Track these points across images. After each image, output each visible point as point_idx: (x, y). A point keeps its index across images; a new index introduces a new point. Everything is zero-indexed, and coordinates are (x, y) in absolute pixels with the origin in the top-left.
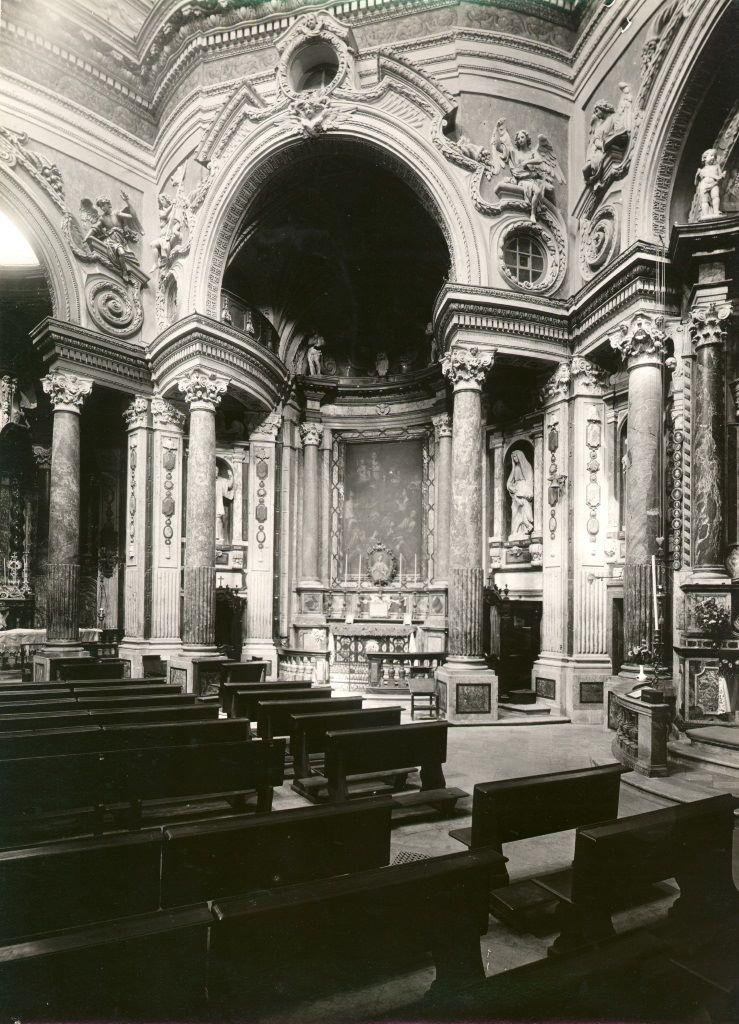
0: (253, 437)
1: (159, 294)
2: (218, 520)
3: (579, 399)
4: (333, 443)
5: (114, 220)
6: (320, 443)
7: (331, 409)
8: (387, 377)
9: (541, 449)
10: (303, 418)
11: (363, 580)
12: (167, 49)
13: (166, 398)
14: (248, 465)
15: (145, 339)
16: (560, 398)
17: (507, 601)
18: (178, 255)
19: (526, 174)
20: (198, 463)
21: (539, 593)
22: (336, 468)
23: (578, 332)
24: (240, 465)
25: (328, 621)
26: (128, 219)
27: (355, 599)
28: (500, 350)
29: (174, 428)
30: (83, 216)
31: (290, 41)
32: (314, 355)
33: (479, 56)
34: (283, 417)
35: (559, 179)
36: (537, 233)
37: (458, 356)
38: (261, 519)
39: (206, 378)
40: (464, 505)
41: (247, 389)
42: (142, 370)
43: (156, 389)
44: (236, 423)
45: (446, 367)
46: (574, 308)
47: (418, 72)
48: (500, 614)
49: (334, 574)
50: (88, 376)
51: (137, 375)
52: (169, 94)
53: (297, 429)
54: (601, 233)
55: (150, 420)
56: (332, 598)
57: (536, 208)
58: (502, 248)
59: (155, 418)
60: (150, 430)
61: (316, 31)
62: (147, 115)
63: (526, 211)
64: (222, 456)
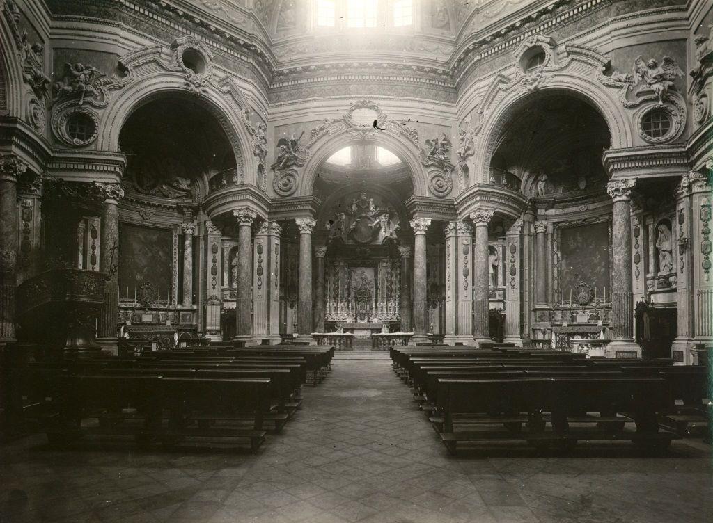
0: (508, 233)
1: (460, 172)
2: (490, 276)
3: (694, 195)
4: (554, 230)
5: (439, 145)
6: (546, 231)
7: (551, 212)
8: (585, 190)
9: (676, 226)
10: (535, 219)
11: (573, 303)
12: (462, 63)
13: (464, 221)
14: (505, 247)
15: (454, 195)
16: (684, 195)
17: (653, 309)
18: (468, 155)
19: (654, 81)
20: (480, 251)
21: (675, 304)
22: (556, 243)
23: (693, 158)
24: (501, 248)
25: (552, 326)
26: (446, 144)
27: (568, 314)
28: (640, 177)
29: (468, 234)
30: (427, 147)
31: (520, 50)
32: (541, 185)
33: (624, 28)
34: (524, 221)
35: (680, 75)
36: (665, 109)
37: (614, 185)
38: (513, 273)
39: (482, 211)
40: (620, 260)
41: (502, 211)
42: (452, 210)
43: (459, 217)
44: (498, 227)
45: (609, 190)
46: (688, 147)
47: (583, 48)
48: (649, 316)
49: (555, 298)
50: (429, 217)
51: (449, 212)
52: (463, 80)
53: (532, 225)
54: (702, 105)
55: (456, 232)
56: (554, 313)
57: (662, 97)
58: (641, 124)
59: (459, 231)
60: (457, 237)
61: (534, 44)
62: (453, 90)
63: (657, 99)
64: (491, 244)
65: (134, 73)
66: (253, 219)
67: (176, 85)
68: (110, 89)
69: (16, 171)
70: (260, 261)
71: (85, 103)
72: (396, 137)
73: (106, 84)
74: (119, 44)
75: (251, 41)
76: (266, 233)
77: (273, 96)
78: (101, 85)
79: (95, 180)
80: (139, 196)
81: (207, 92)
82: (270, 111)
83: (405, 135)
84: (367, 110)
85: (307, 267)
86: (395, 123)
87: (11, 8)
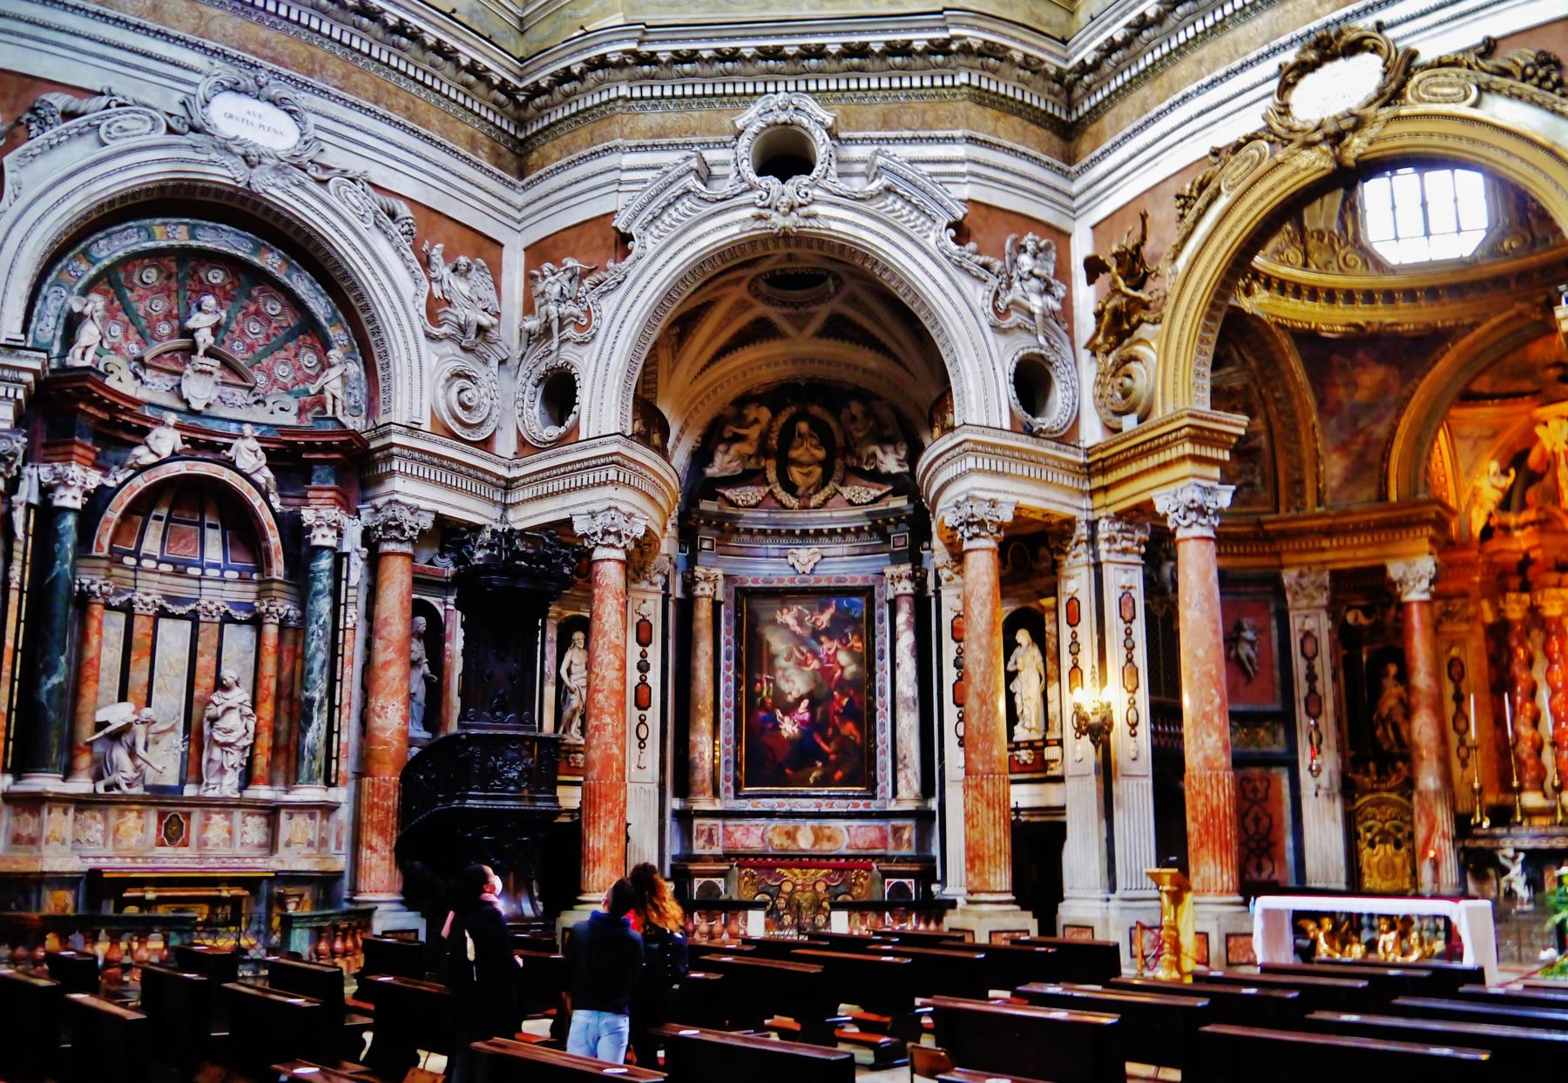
65: (649, 239)
66: (1000, 527)
67: (735, 229)
69: (403, 532)
70: (1074, 649)
72: (1463, 109)
75: (946, 29)
76: (1084, 558)
77: (1085, 145)
79: (572, 511)
80: (786, 515)
81: (814, 216)
82: (1075, 188)
83: (1499, 92)
84: (1341, 63)
85: (1200, 653)
86: (1455, 63)
87: (392, 215)
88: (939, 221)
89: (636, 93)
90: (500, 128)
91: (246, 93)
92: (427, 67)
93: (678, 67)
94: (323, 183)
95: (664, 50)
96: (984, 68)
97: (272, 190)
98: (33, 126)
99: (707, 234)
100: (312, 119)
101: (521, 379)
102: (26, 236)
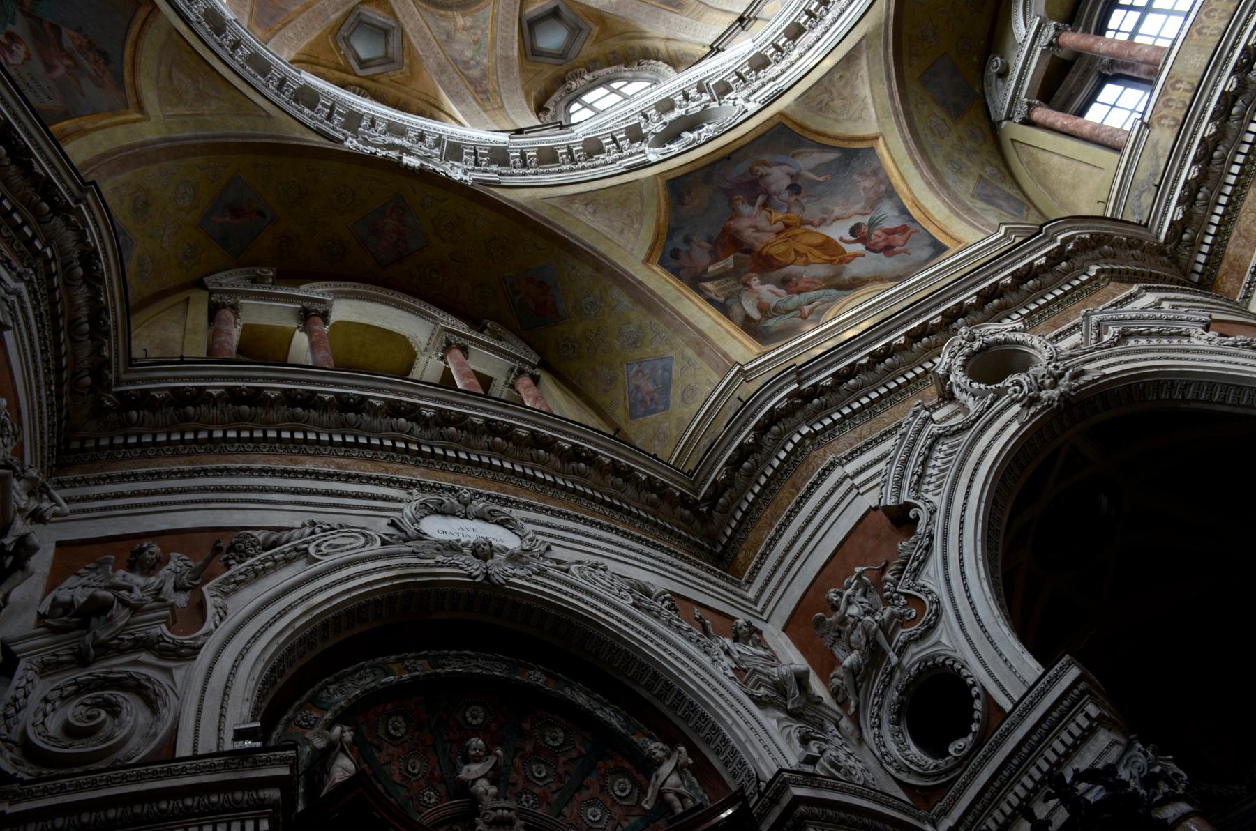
65: (929, 496)
67: (1015, 426)
68: (916, 573)
71: (900, 653)
73: (901, 572)
74: (861, 491)
75: (1054, 241)
78: (895, 586)
88: (1193, 332)
89: (818, 427)
90: (696, 544)
91: (454, 515)
92: (610, 490)
93: (845, 386)
94: (567, 571)
95: (824, 377)
96: (1104, 256)
97: (512, 580)
98: (232, 562)
99: (989, 446)
100: (528, 527)
101: (868, 735)
102: (241, 655)
